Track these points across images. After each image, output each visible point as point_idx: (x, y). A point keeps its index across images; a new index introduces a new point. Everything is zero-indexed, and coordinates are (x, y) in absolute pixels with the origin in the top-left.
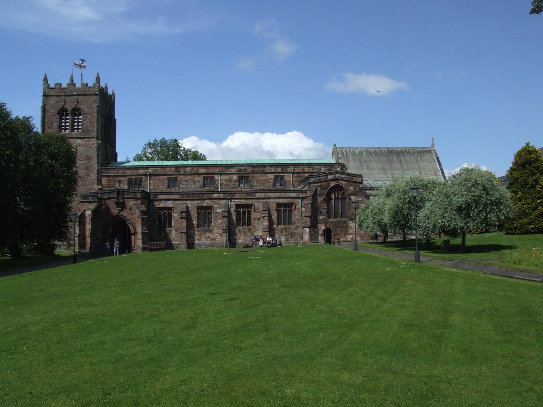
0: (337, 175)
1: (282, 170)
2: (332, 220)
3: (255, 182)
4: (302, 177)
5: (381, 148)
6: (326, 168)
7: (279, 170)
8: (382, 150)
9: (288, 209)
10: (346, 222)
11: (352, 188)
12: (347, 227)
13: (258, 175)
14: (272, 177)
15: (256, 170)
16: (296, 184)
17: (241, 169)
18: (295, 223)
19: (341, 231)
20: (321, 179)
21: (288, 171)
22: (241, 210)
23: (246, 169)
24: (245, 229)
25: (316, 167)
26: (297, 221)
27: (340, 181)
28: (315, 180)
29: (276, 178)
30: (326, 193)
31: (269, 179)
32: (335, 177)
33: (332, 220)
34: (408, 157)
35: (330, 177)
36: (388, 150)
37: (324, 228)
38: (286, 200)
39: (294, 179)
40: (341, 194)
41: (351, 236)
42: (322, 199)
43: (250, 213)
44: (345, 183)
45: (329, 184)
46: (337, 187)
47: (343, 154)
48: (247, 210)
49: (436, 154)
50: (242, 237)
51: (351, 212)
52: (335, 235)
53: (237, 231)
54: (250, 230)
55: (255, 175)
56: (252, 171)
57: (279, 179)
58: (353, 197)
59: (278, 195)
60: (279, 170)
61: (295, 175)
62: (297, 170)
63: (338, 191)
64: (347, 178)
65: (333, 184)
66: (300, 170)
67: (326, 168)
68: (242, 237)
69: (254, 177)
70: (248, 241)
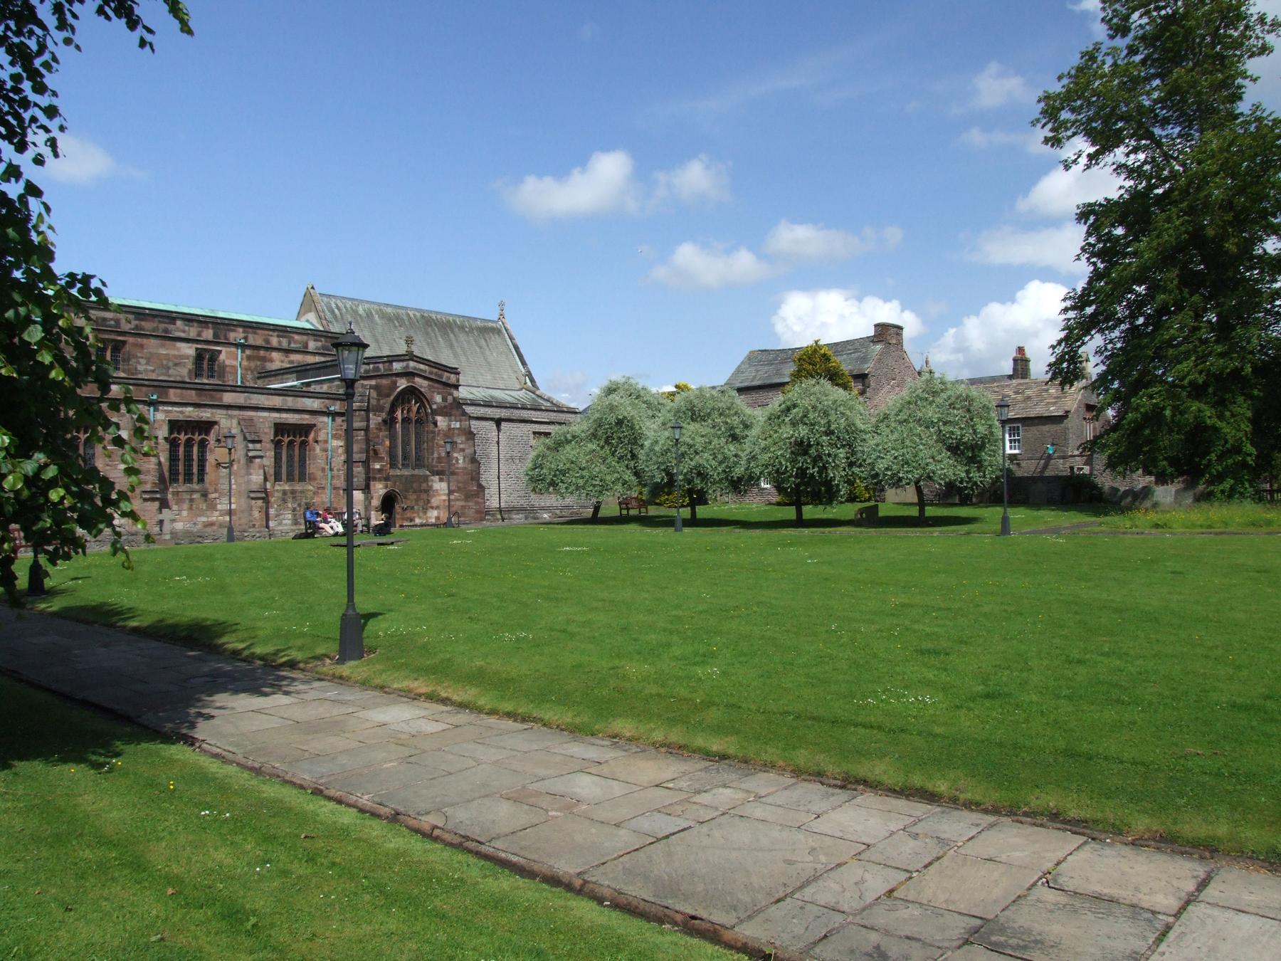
0: (412, 364)
1: (215, 335)
2: (398, 472)
3: (143, 361)
4: (264, 359)
5: (406, 308)
6: (319, 344)
7: (208, 334)
8: (411, 313)
9: (298, 440)
10: (426, 479)
11: (438, 399)
12: (428, 491)
13: (153, 341)
14: (189, 350)
15: (148, 325)
16: (249, 377)
17: (104, 319)
18: (315, 479)
19: (417, 501)
20: (377, 369)
21: (232, 341)
22: (183, 437)
23: (118, 321)
24: (193, 491)
25: (297, 337)
26: (319, 474)
27: (417, 380)
28: (366, 371)
29: (199, 356)
30: (388, 406)
31: (181, 357)
32: (407, 367)
33: (398, 472)
34: (462, 337)
35: (397, 366)
36: (422, 316)
37: (382, 492)
38: (297, 416)
39: (245, 363)
40: (415, 409)
41: (435, 513)
42: (380, 419)
43: (203, 445)
44: (425, 383)
45: (394, 385)
46: (412, 392)
47: (333, 312)
48: (197, 438)
49: (511, 338)
50: (185, 513)
51: (436, 455)
52: (404, 510)
53: (170, 496)
54: (205, 495)
55: (145, 341)
56: (137, 327)
57: (205, 361)
58: (442, 422)
59: (277, 401)
60: (208, 334)
61: (248, 352)
62: (251, 341)
63: (409, 402)
64: (431, 373)
65: (402, 384)
66: (260, 342)
67: (319, 344)
68: (185, 513)
69: (142, 346)
70: (200, 526)
